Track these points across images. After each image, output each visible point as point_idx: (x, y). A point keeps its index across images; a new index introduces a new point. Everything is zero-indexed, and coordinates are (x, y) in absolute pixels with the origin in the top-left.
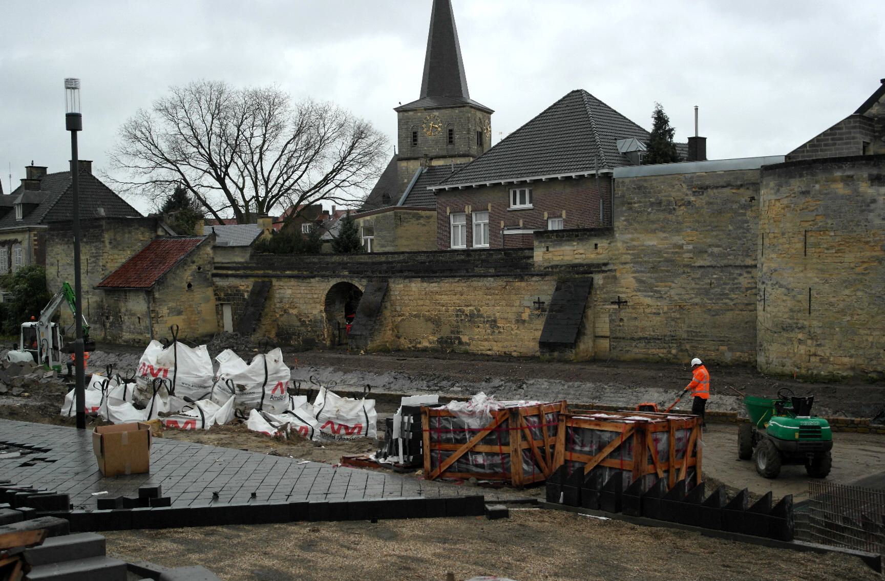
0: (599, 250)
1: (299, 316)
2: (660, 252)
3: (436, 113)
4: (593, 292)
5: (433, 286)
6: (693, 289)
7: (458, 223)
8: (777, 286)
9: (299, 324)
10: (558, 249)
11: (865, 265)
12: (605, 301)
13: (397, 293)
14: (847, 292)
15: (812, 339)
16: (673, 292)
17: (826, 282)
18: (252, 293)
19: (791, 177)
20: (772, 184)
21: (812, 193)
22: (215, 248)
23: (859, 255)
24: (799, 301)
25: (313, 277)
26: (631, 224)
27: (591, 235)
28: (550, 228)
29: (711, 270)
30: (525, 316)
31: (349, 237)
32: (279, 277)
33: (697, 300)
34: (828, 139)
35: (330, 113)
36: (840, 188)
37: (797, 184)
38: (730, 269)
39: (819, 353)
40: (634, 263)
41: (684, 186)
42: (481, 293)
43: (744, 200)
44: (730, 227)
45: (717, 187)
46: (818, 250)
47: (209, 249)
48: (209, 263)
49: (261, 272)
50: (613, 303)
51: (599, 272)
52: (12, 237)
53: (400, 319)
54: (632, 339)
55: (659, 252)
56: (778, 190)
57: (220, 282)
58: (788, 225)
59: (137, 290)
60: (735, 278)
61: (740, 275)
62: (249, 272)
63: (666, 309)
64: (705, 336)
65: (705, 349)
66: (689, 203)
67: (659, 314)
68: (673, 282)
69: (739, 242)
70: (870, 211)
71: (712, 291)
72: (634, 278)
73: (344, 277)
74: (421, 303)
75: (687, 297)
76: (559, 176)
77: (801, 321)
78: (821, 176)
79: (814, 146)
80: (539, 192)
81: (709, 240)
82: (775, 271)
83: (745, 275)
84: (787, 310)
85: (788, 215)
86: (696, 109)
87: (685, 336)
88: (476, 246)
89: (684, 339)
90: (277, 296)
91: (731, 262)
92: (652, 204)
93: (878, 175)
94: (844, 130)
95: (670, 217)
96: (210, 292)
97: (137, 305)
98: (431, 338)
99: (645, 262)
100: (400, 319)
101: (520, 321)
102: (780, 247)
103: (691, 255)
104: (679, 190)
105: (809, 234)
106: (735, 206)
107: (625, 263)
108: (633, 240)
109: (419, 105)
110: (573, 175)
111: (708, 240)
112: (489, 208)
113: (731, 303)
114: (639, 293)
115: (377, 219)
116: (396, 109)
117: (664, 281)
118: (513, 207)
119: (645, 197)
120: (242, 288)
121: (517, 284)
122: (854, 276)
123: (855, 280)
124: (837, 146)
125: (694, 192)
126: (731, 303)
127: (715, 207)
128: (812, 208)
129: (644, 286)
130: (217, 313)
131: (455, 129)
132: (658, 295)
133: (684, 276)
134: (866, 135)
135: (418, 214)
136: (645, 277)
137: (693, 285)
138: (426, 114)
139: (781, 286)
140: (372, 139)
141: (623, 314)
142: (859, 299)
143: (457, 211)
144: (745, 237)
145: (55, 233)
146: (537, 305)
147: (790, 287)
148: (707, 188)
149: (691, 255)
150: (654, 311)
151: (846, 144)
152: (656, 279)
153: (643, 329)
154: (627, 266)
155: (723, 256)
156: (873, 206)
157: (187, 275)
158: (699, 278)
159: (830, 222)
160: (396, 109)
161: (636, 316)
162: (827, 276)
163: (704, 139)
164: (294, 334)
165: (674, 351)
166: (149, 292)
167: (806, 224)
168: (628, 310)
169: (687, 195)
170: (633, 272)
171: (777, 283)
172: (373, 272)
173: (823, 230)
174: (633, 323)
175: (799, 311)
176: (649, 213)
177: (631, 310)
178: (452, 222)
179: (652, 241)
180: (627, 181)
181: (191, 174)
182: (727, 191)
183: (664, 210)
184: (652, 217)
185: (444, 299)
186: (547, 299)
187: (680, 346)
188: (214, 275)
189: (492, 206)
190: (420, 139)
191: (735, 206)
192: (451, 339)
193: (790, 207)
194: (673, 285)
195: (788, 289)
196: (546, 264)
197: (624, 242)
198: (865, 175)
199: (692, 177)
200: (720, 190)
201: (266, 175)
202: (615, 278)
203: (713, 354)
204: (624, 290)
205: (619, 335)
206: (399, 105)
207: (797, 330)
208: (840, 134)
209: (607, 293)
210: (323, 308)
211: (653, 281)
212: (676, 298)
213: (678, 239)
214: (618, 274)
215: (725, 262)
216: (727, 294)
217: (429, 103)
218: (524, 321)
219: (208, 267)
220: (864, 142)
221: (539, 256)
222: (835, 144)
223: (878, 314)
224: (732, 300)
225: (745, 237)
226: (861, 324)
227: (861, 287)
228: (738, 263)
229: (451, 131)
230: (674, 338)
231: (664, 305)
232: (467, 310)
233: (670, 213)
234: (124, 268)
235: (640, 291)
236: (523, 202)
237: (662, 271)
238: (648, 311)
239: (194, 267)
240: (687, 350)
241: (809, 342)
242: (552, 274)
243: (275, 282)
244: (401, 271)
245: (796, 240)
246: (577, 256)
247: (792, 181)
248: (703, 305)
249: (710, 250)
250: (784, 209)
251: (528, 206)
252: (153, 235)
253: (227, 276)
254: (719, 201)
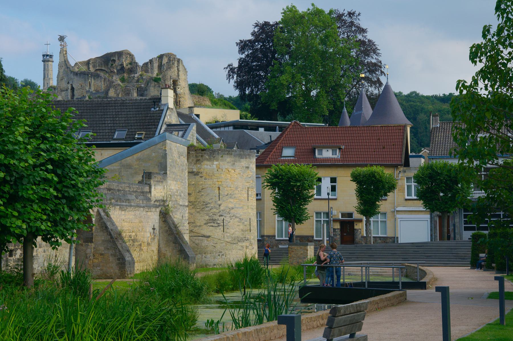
8: (234, 217)
19: (241, 158)
20: (228, 160)
24: (246, 226)
56: (234, 164)
77: (247, 236)
82: (232, 208)
128: (249, 176)
139: (236, 217)
147: (241, 217)
167: (248, 184)
171: (234, 216)
193: (240, 174)
195: (241, 219)
241: (250, 247)
247: (242, 160)
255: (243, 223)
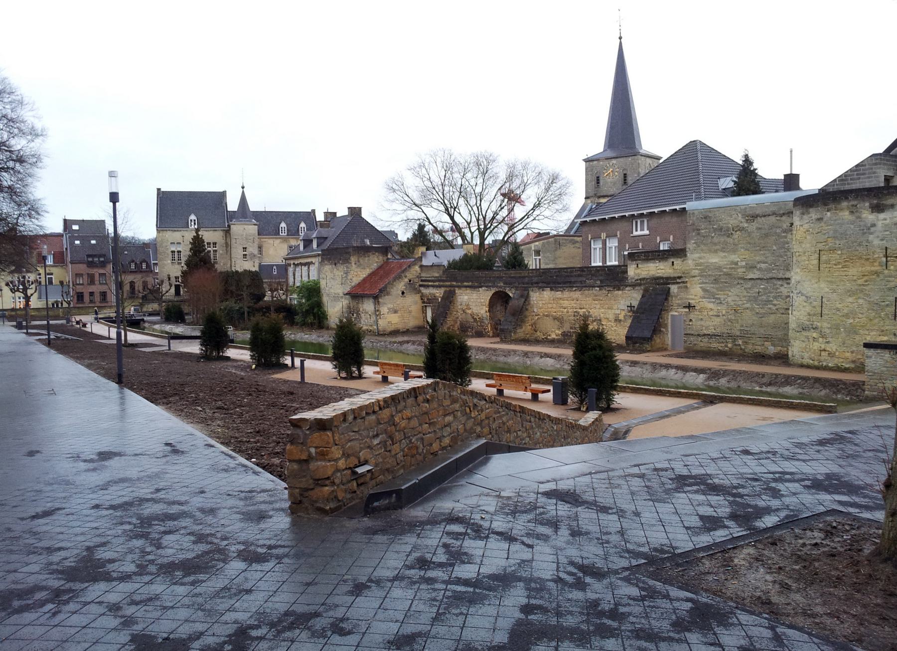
0: (676, 267)
1: (472, 315)
2: (721, 267)
3: (614, 161)
4: (670, 298)
5: (559, 294)
6: (745, 296)
7: (597, 246)
9: (472, 320)
10: (646, 265)
11: (866, 278)
12: (679, 305)
13: (534, 299)
14: (850, 299)
15: (823, 337)
16: (730, 299)
17: (834, 291)
18: (442, 298)
21: (825, 219)
22: (421, 266)
23: (860, 269)
24: (814, 307)
25: (481, 287)
26: (699, 246)
27: (669, 255)
28: (661, 248)
29: (759, 281)
30: (621, 317)
31: (515, 258)
32: (459, 287)
33: (748, 305)
34: (853, 175)
35: (531, 165)
36: (846, 215)
37: (814, 214)
38: (775, 282)
39: (828, 349)
40: (702, 276)
41: (740, 215)
42: (591, 299)
43: (785, 225)
44: (775, 248)
45: (765, 216)
46: (828, 266)
47: (417, 268)
48: (418, 277)
49: (449, 283)
50: (685, 307)
51: (674, 283)
52: (309, 260)
53: (537, 317)
54: (699, 335)
55: (719, 268)
57: (425, 291)
58: (808, 245)
59: (367, 296)
60: (778, 288)
61: (782, 285)
62: (441, 283)
63: (724, 312)
64: (753, 334)
65: (753, 344)
66: (742, 229)
67: (719, 316)
68: (730, 291)
69: (781, 259)
70: (872, 234)
71: (760, 298)
72: (701, 287)
73: (501, 287)
74: (550, 306)
75: (740, 303)
76: (667, 209)
77: (815, 323)
78: (832, 206)
79: (842, 180)
80: (655, 221)
81: (758, 258)
83: (786, 285)
84: (806, 314)
85: (808, 237)
86: (791, 151)
87: (738, 333)
88: (608, 264)
89: (738, 336)
90: (459, 300)
91: (774, 276)
92: (715, 230)
93: (877, 203)
94: (867, 167)
95: (730, 240)
96: (417, 298)
97: (368, 306)
98: (557, 332)
99: (709, 275)
100: (537, 317)
101: (617, 320)
102: (802, 263)
103: (744, 270)
104: (735, 219)
105: (822, 253)
106: (778, 231)
107: (694, 277)
108: (700, 258)
109: (601, 156)
110: (678, 207)
111: (757, 258)
112: (618, 234)
113: (774, 308)
114: (704, 300)
115: (543, 245)
116: (585, 160)
117: (723, 291)
118: (635, 233)
119: (710, 224)
120: (437, 295)
121: (616, 292)
122: (856, 287)
123: (857, 290)
124: (861, 180)
125: (747, 220)
126: (774, 308)
127: (763, 232)
129: (709, 294)
130: (423, 312)
131: (628, 173)
132: (718, 301)
133: (739, 286)
134: (888, 169)
135: (573, 240)
136: (708, 287)
137: (745, 294)
138: (607, 162)
139: (803, 295)
140: (564, 182)
141: (692, 316)
142: (860, 306)
143: (596, 237)
144: (786, 255)
145: (325, 257)
146: (629, 308)
147: (808, 295)
148: (757, 216)
149: (744, 270)
150: (715, 314)
151: (869, 178)
152: (717, 289)
153: (707, 328)
154: (696, 279)
155: (769, 270)
156: (872, 229)
157: (401, 286)
158: (750, 288)
159: (837, 242)
160: (585, 160)
161: (700, 317)
162: (834, 287)
163: (798, 175)
164: (469, 327)
165: (730, 345)
166: (376, 298)
168: (695, 313)
169: (741, 222)
170: (700, 284)
172: (519, 284)
173: (833, 250)
174: (699, 323)
175: (814, 315)
176: (713, 237)
177: (698, 313)
178: (592, 246)
179: (714, 259)
180: (695, 212)
181: (431, 213)
182: (773, 219)
183: (724, 235)
184: (716, 240)
185: (566, 303)
186: (635, 303)
187: (735, 341)
188: (421, 286)
189: (620, 234)
190: (601, 182)
191: (778, 231)
192: (570, 332)
194: (730, 294)
196: (636, 278)
197: (694, 260)
198: (867, 204)
199: (746, 208)
200: (767, 218)
201: (484, 214)
202: (686, 287)
203: (759, 347)
204: (693, 297)
205: (689, 332)
206: (586, 157)
207: (813, 331)
208: (863, 170)
209: (681, 299)
210: (487, 309)
211: (714, 290)
212: (732, 304)
213: (734, 257)
214: (688, 285)
215: (770, 275)
216: (771, 301)
217: (610, 154)
218: (620, 321)
219: (416, 280)
220: (885, 176)
221: (633, 271)
222: (859, 178)
223: (875, 318)
224: (775, 305)
225: (786, 255)
226: (863, 326)
227: (861, 295)
228: (780, 276)
229: (625, 175)
230: (730, 336)
231: (723, 309)
232: (581, 312)
233: (728, 236)
234: (365, 280)
235: (705, 298)
236: (642, 229)
237: (722, 282)
238: (711, 313)
239: (406, 280)
240: (739, 345)
241: (821, 339)
242: (640, 285)
243: (457, 291)
244: (537, 283)
245: (812, 257)
246: (659, 271)
247: (811, 210)
248: (752, 309)
249: (758, 266)
250: (805, 232)
251: (646, 232)
252: (385, 258)
253: (428, 286)
254: (766, 226)
255: (811, 303)
